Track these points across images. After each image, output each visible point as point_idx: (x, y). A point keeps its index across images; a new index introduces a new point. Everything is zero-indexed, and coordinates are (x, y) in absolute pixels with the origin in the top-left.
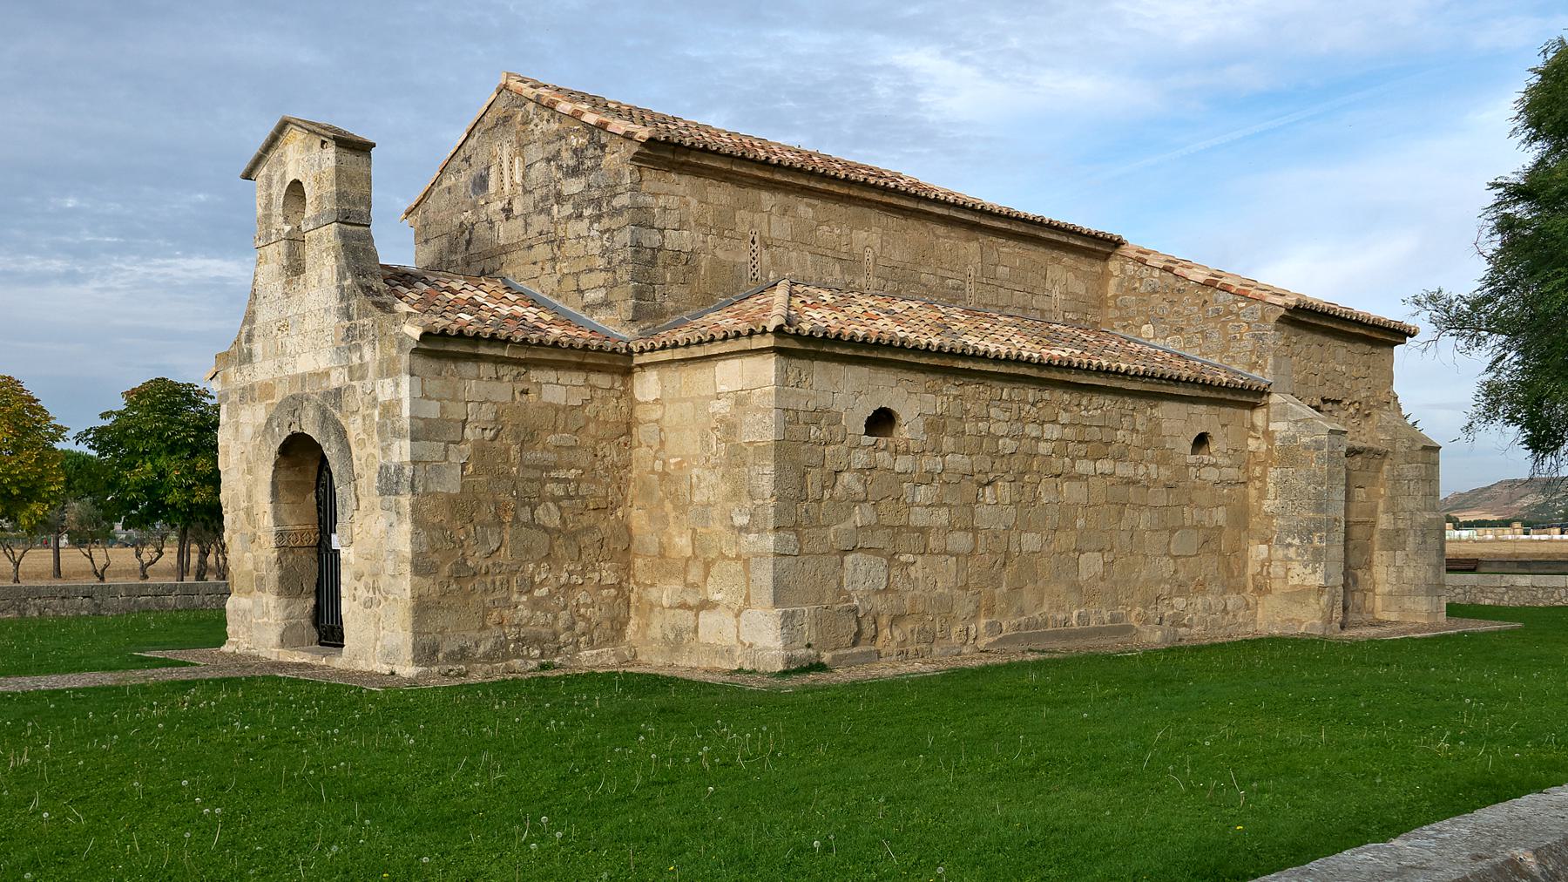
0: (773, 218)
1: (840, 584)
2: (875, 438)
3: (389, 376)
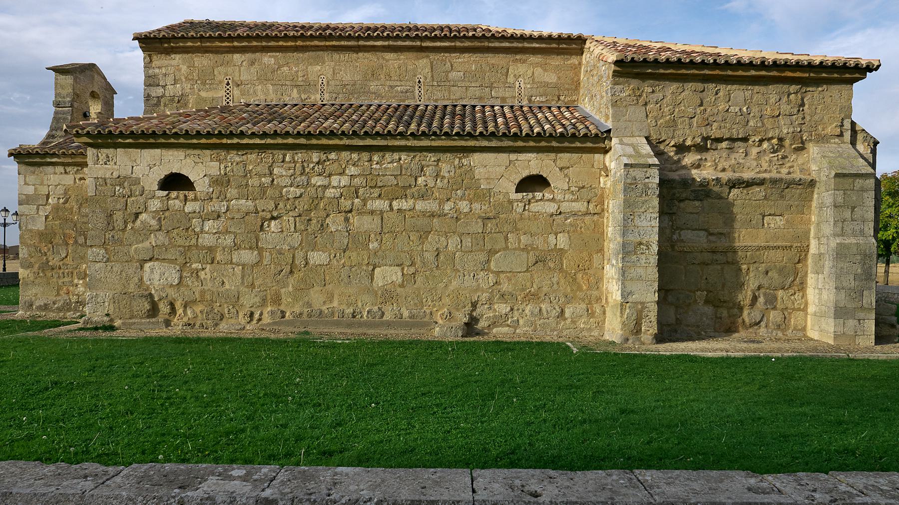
0: (242, 69)
1: (141, 279)
2: (167, 192)
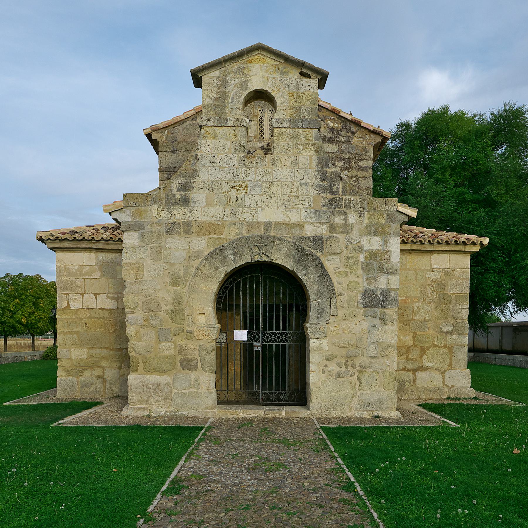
3: (376, 234)
